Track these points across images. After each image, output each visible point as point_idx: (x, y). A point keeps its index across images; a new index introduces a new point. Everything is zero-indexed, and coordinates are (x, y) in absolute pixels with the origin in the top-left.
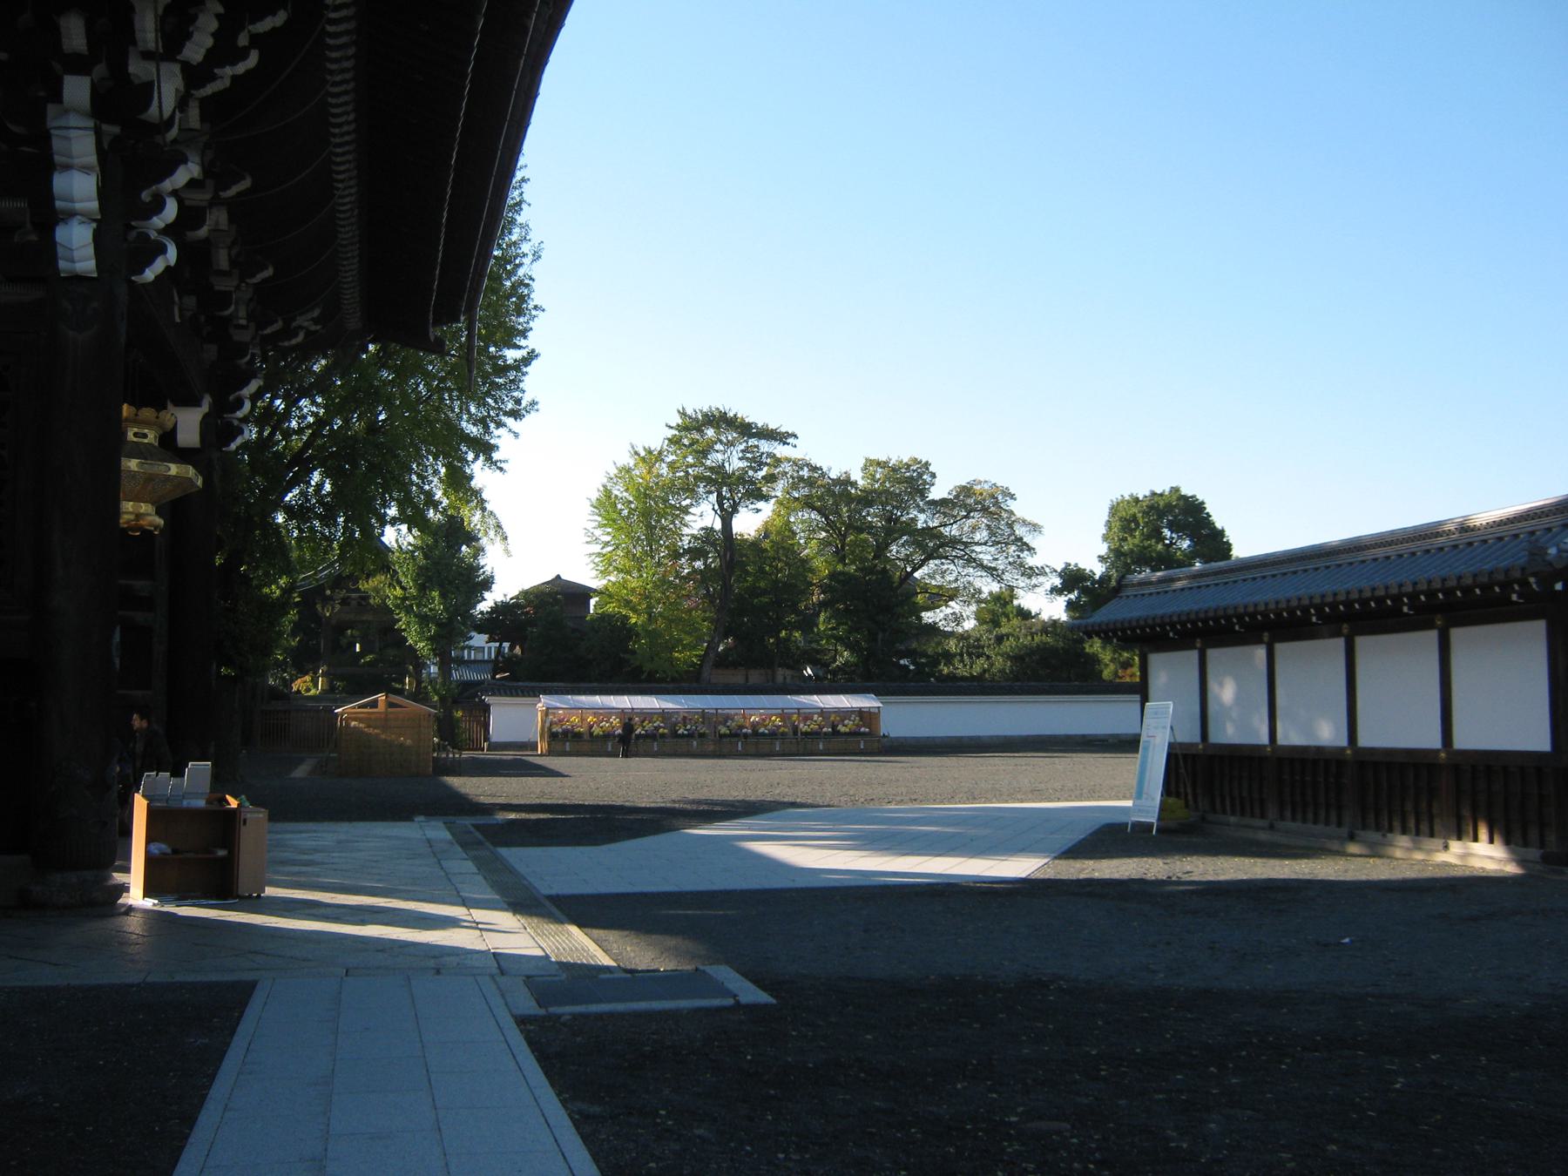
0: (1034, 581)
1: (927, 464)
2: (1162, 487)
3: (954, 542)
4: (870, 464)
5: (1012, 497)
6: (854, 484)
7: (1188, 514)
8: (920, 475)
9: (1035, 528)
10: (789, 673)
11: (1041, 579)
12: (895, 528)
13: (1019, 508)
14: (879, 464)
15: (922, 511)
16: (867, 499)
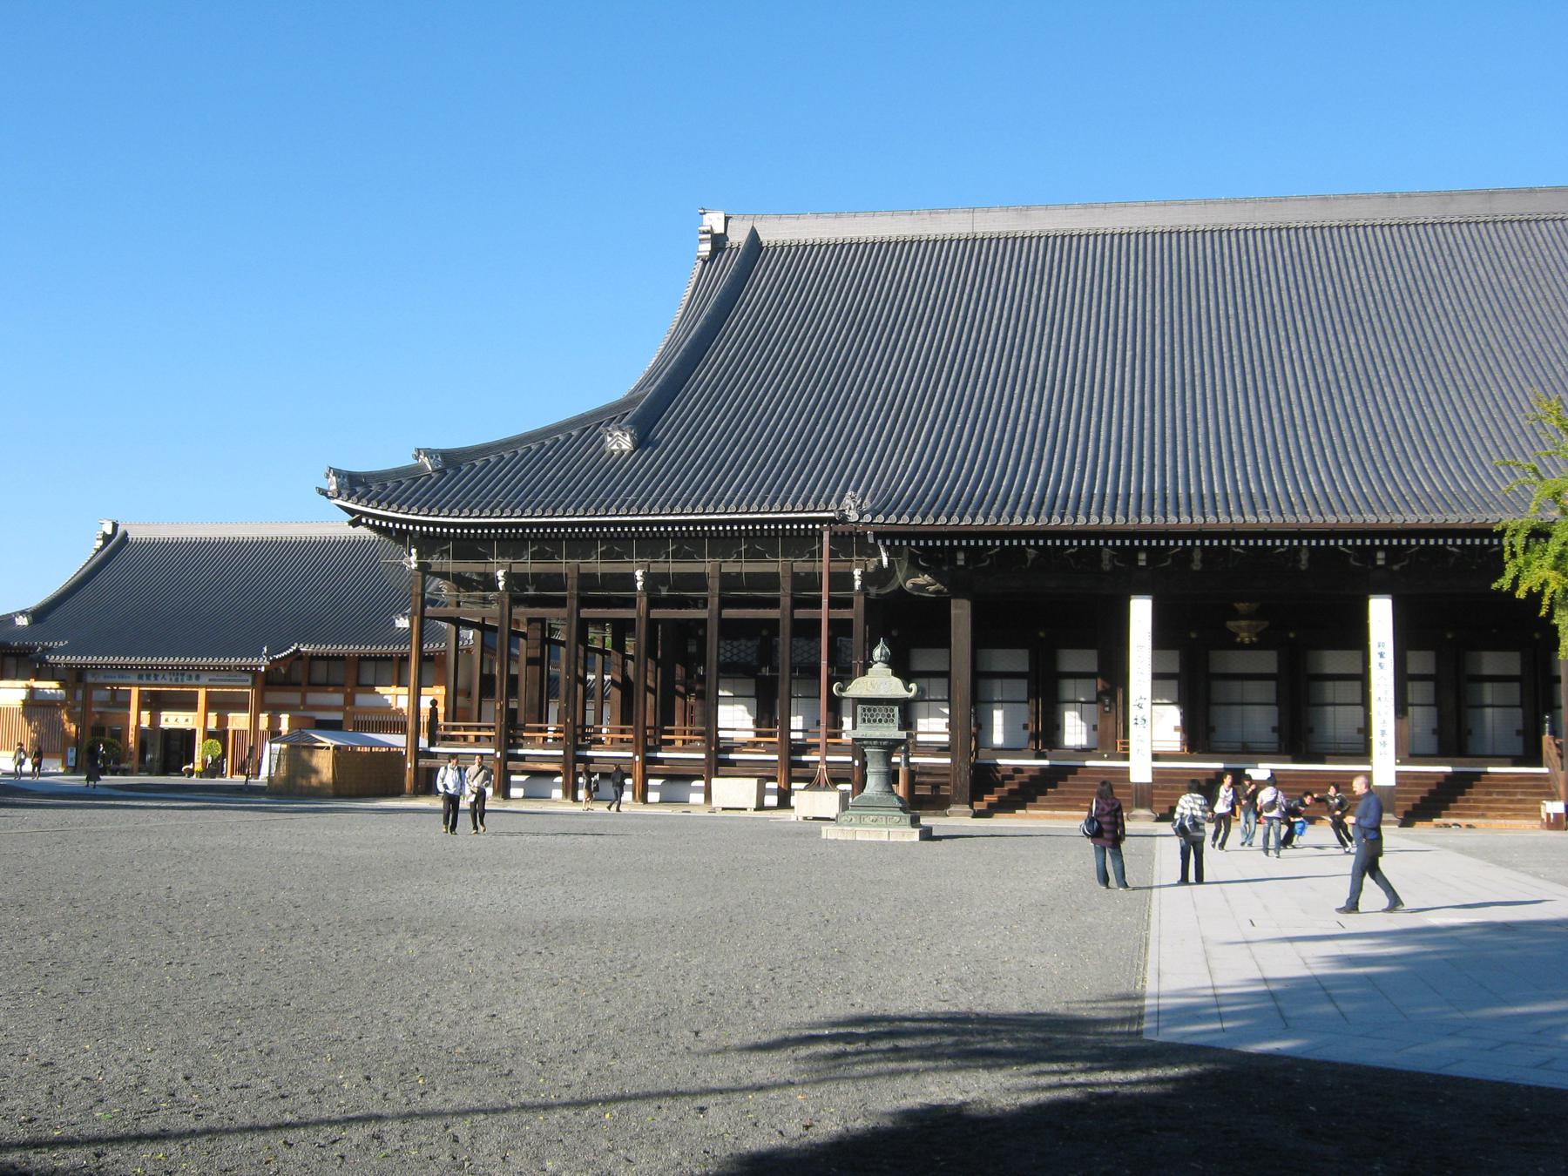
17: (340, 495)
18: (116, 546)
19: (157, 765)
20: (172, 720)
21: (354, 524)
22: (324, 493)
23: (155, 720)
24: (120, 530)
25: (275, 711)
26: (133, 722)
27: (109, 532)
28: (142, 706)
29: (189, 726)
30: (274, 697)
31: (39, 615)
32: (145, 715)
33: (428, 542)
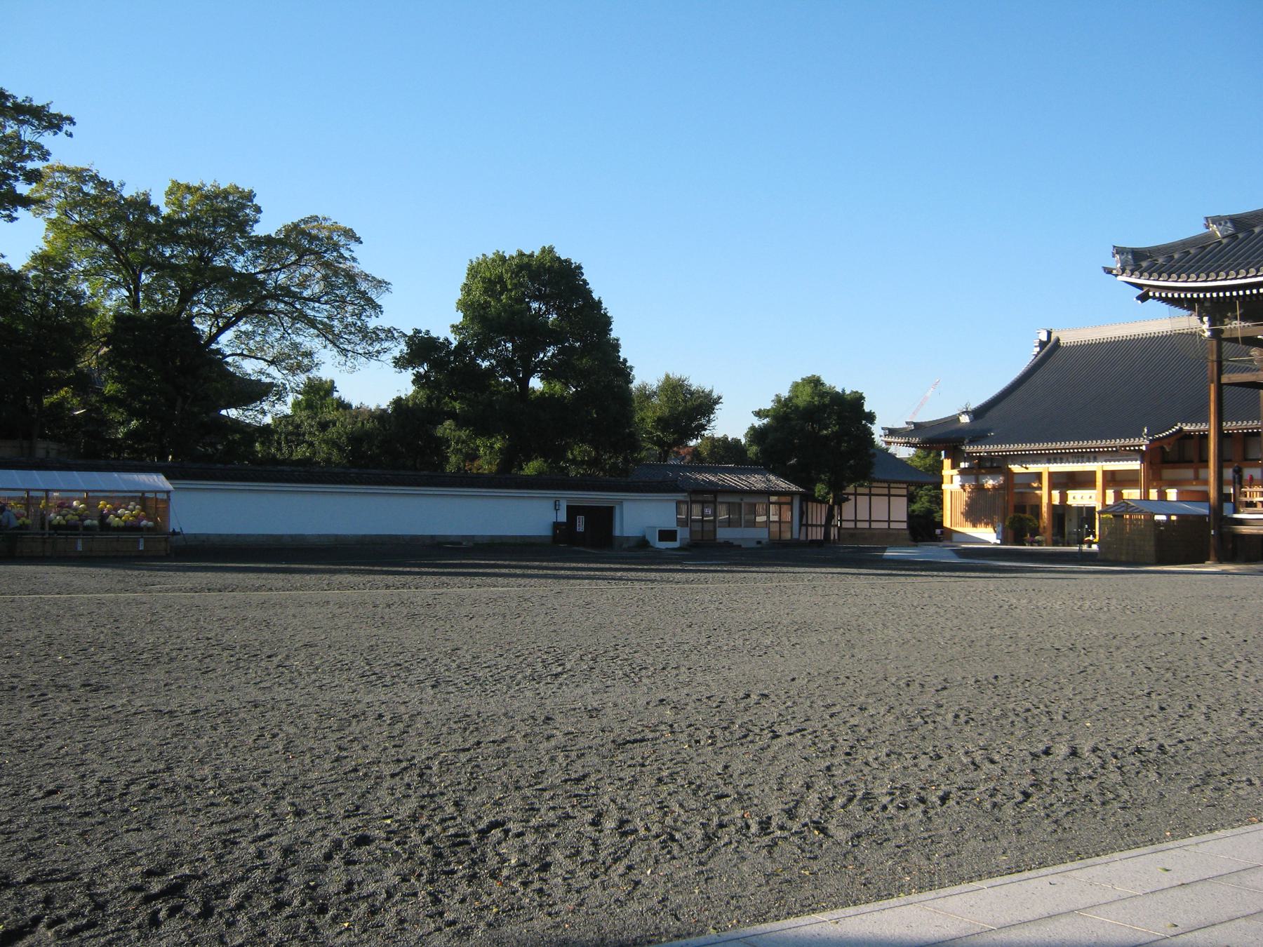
0: (377, 347)
1: (250, 196)
2: (533, 247)
3: (284, 293)
4: (177, 190)
5: (358, 240)
6: (156, 211)
7: (558, 280)
8: (243, 207)
9: (380, 284)
10: (54, 446)
11: (386, 345)
12: (202, 276)
13: (366, 259)
14: (188, 188)
15: (240, 252)
16: (169, 230)
17: (1123, 271)
18: (1051, 349)
19: (1049, 541)
20: (1077, 498)
21: (1144, 298)
22: (1109, 271)
23: (1064, 497)
24: (1053, 338)
25: (1162, 486)
26: (1045, 500)
27: (1044, 338)
28: (1052, 486)
29: (1091, 503)
30: (1168, 473)
31: (977, 414)
32: (1056, 494)
33: (1215, 308)
